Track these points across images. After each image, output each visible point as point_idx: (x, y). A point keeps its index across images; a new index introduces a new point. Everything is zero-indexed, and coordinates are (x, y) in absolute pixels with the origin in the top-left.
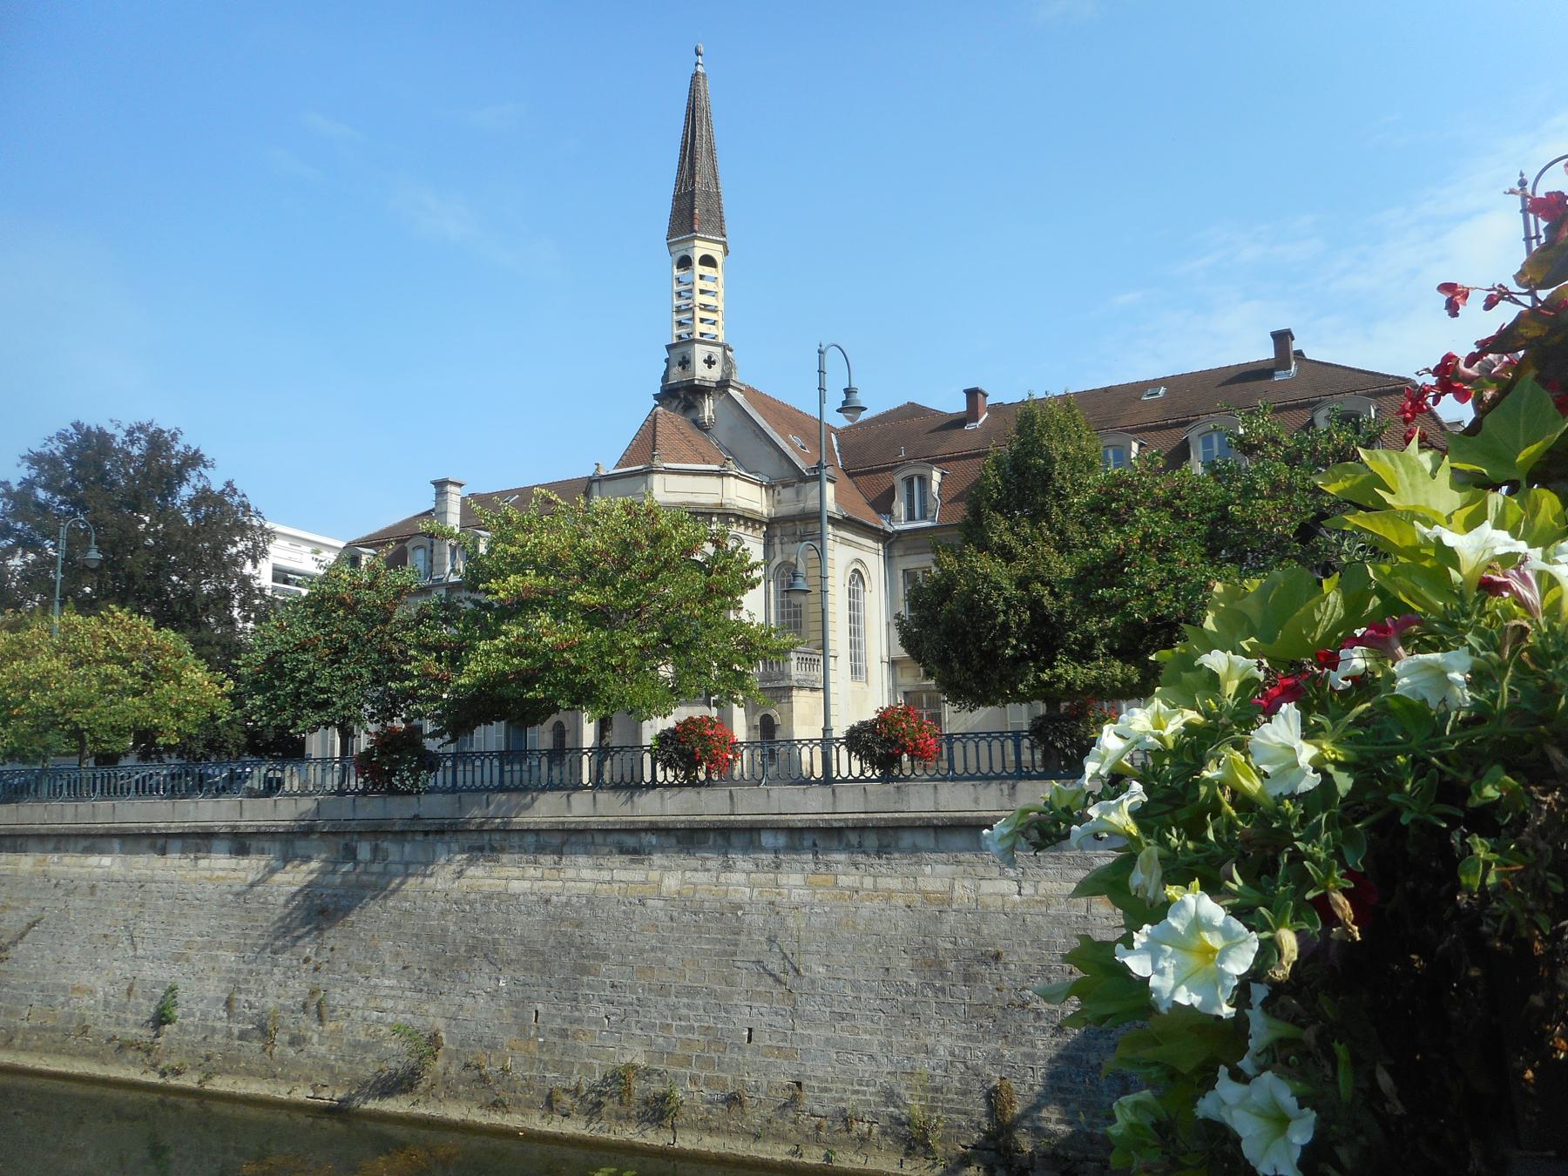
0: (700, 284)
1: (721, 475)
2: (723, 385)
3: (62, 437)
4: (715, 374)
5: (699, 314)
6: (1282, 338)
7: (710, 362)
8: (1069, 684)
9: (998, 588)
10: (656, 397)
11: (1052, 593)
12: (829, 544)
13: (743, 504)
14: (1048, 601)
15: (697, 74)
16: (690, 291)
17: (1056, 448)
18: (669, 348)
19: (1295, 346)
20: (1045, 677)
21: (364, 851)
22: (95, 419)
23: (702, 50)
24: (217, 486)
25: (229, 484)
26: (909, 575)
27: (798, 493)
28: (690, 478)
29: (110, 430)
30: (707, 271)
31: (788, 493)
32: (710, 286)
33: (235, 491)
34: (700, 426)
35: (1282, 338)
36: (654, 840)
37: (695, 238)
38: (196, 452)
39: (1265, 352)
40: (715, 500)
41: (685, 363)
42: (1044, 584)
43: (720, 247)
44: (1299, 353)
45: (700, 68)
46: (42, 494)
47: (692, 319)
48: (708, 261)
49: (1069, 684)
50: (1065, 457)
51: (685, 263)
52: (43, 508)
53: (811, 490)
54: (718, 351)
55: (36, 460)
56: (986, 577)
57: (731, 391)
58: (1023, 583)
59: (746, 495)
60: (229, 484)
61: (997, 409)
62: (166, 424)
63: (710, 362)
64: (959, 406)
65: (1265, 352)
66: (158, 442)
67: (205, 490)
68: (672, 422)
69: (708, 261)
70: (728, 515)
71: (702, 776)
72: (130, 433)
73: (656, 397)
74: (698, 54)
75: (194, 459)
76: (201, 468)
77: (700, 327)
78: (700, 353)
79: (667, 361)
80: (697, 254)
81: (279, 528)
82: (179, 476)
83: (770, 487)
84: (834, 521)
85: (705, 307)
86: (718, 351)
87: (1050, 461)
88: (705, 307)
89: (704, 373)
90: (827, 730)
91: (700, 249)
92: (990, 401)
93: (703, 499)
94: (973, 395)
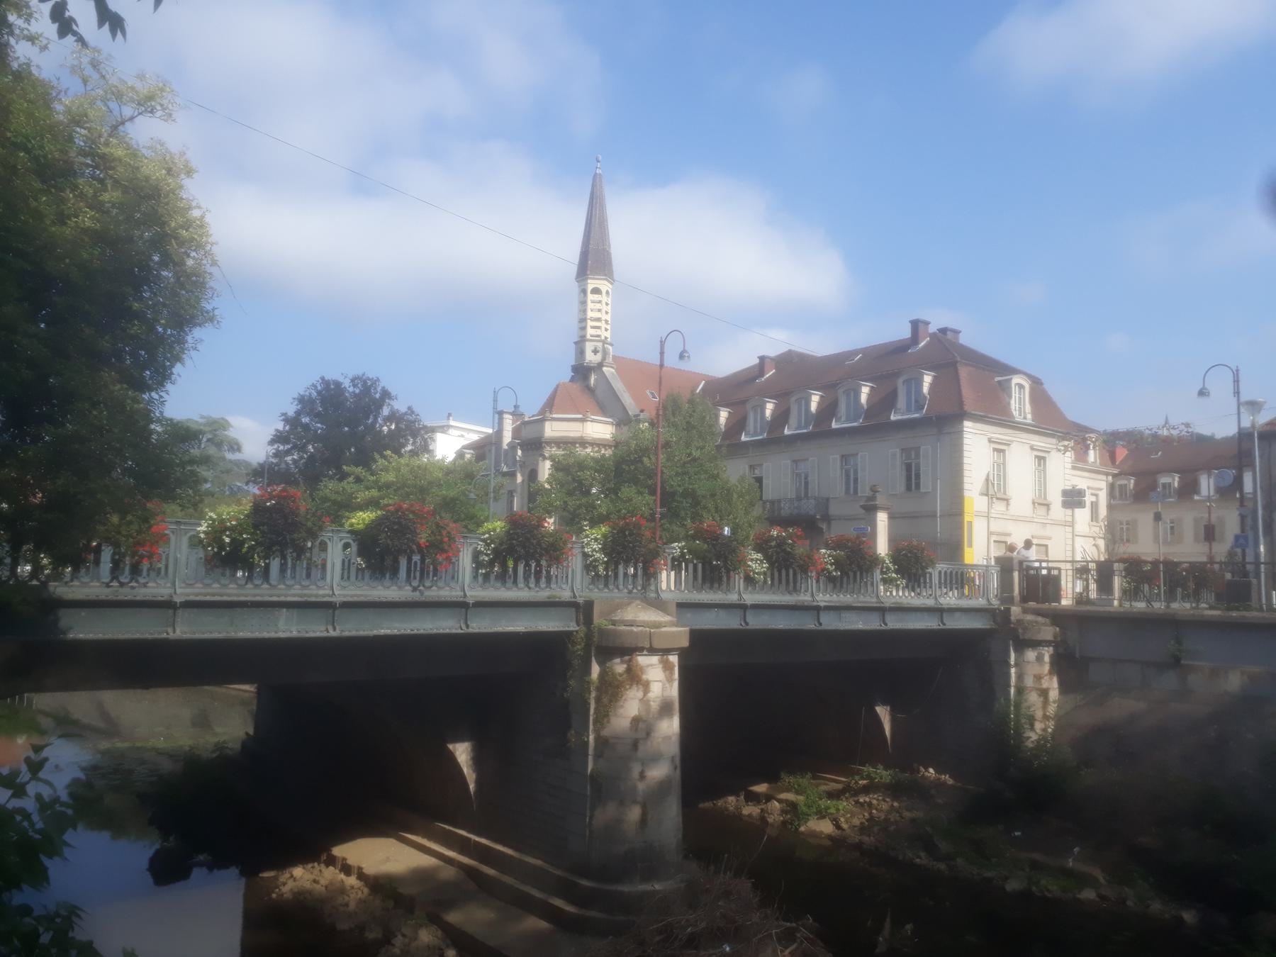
1: (583, 420)
2: (600, 365)
3: (314, 386)
4: (598, 358)
5: (590, 323)
7: (595, 352)
22: (333, 375)
25: (409, 408)
28: (565, 424)
29: (341, 379)
30: (596, 297)
39: (906, 333)
41: (581, 353)
46: (305, 420)
48: (596, 291)
51: (584, 292)
52: (306, 427)
54: (600, 345)
55: (301, 400)
62: (371, 374)
66: (366, 386)
69: (596, 291)
72: (352, 381)
75: (386, 394)
78: (589, 347)
80: (590, 287)
82: (379, 405)
89: (591, 358)
91: (591, 284)
93: (572, 435)
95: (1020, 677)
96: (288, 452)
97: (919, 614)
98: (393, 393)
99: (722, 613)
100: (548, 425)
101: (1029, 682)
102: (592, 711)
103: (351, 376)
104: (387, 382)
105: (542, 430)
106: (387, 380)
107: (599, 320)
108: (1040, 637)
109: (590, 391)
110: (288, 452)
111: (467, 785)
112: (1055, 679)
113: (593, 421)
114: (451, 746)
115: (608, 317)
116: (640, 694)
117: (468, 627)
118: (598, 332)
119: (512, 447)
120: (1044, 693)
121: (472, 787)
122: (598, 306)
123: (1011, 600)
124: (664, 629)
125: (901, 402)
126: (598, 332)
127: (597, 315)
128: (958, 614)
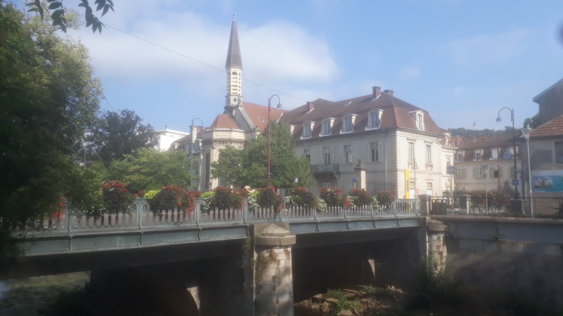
1: (230, 131)
2: (237, 106)
4: (236, 103)
5: (232, 88)
7: (235, 100)
13: (237, 138)
15: (233, 22)
25: (148, 124)
29: (117, 112)
30: (234, 76)
31: (249, 135)
34: (232, 116)
41: (228, 101)
45: (234, 20)
46: (100, 130)
51: (229, 74)
52: (101, 134)
54: (237, 97)
62: (131, 109)
63: (235, 100)
66: (128, 114)
69: (235, 73)
72: (122, 112)
75: (138, 118)
77: (234, 91)
78: (232, 98)
80: (232, 72)
82: (134, 123)
83: (246, 133)
86: (237, 97)
89: (233, 103)
91: (232, 70)
95: (431, 246)
96: (93, 145)
97: (388, 222)
98: (141, 118)
99: (308, 226)
100: (214, 133)
101: (434, 249)
102: (254, 274)
103: (121, 110)
104: (138, 113)
105: (212, 135)
106: (138, 113)
107: (236, 86)
108: (439, 229)
109: (233, 117)
110: (93, 145)
111: (196, 306)
112: (445, 247)
113: (235, 131)
114: (188, 289)
115: (240, 85)
116: (276, 266)
117: (199, 239)
118: (236, 91)
119: (197, 142)
120: (441, 253)
121: (198, 306)
122: (236, 80)
123: (425, 214)
124: (286, 237)
125: (370, 123)
126: (236, 91)
128: (404, 221)
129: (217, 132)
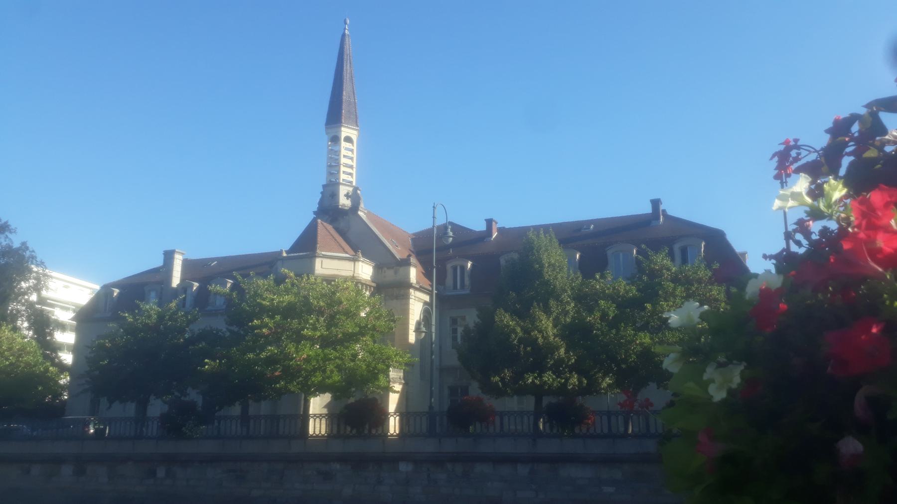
0: (343, 152)
1: (354, 260)
5: (343, 169)
6: (656, 203)
8: (550, 386)
9: (516, 333)
10: (315, 213)
11: (543, 337)
12: (411, 301)
14: (540, 341)
15: (344, 35)
16: (339, 155)
17: (545, 261)
18: (324, 186)
19: (662, 207)
20: (537, 382)
21: (161, 473)
23: (348, 22)
24: (16, 245)
25: (24, 244)
26: (454, 321)
27: (396, 273)
30: (348, 145)
32: (349, 154)
33: (27, 248)
35: (656, 203)
36: (338, 466)
37: (341, 126)
38: (6, 223)
40: (350, 274)
41: (334, 195)
42: (540, 331)
43: (355, 132)
44: (664, 211)
45: (347, 32)
47: (339, 172)
48: (348, 139)
49: (550, 386)
50: (550, 264)
51: (335, 140)
53: (402, 270)
56: (508, 326)
57: (360, 213)
58: (526, 331)
59: (365, 271)
60: (24, 244)
61: (501, 230)
64: (481, 227)
65: (647, 209)
67: (10, 247)
68: (325, 230)
69: (348, 139)
70: (356, 282)
71: (366, 432)
73: (315, 213)
74: (346, 23)
76: (7, 233)
78: (343, 190)
79: (322, 193)
81: (54, 274)
84: (416, 289)
85: (346, 166)
87: (542, 266)
88: (346, 166)
89: (344, 202)
90: (431, 407)
91: (345, 132)
92: (499, 225)
93: (344, 274)
94: (489, 222)
98: (13, 227)
100: (318, 261)
107: (351, 167)
118: (349, 178)
127: (349, 162)
129: (325, 261)
